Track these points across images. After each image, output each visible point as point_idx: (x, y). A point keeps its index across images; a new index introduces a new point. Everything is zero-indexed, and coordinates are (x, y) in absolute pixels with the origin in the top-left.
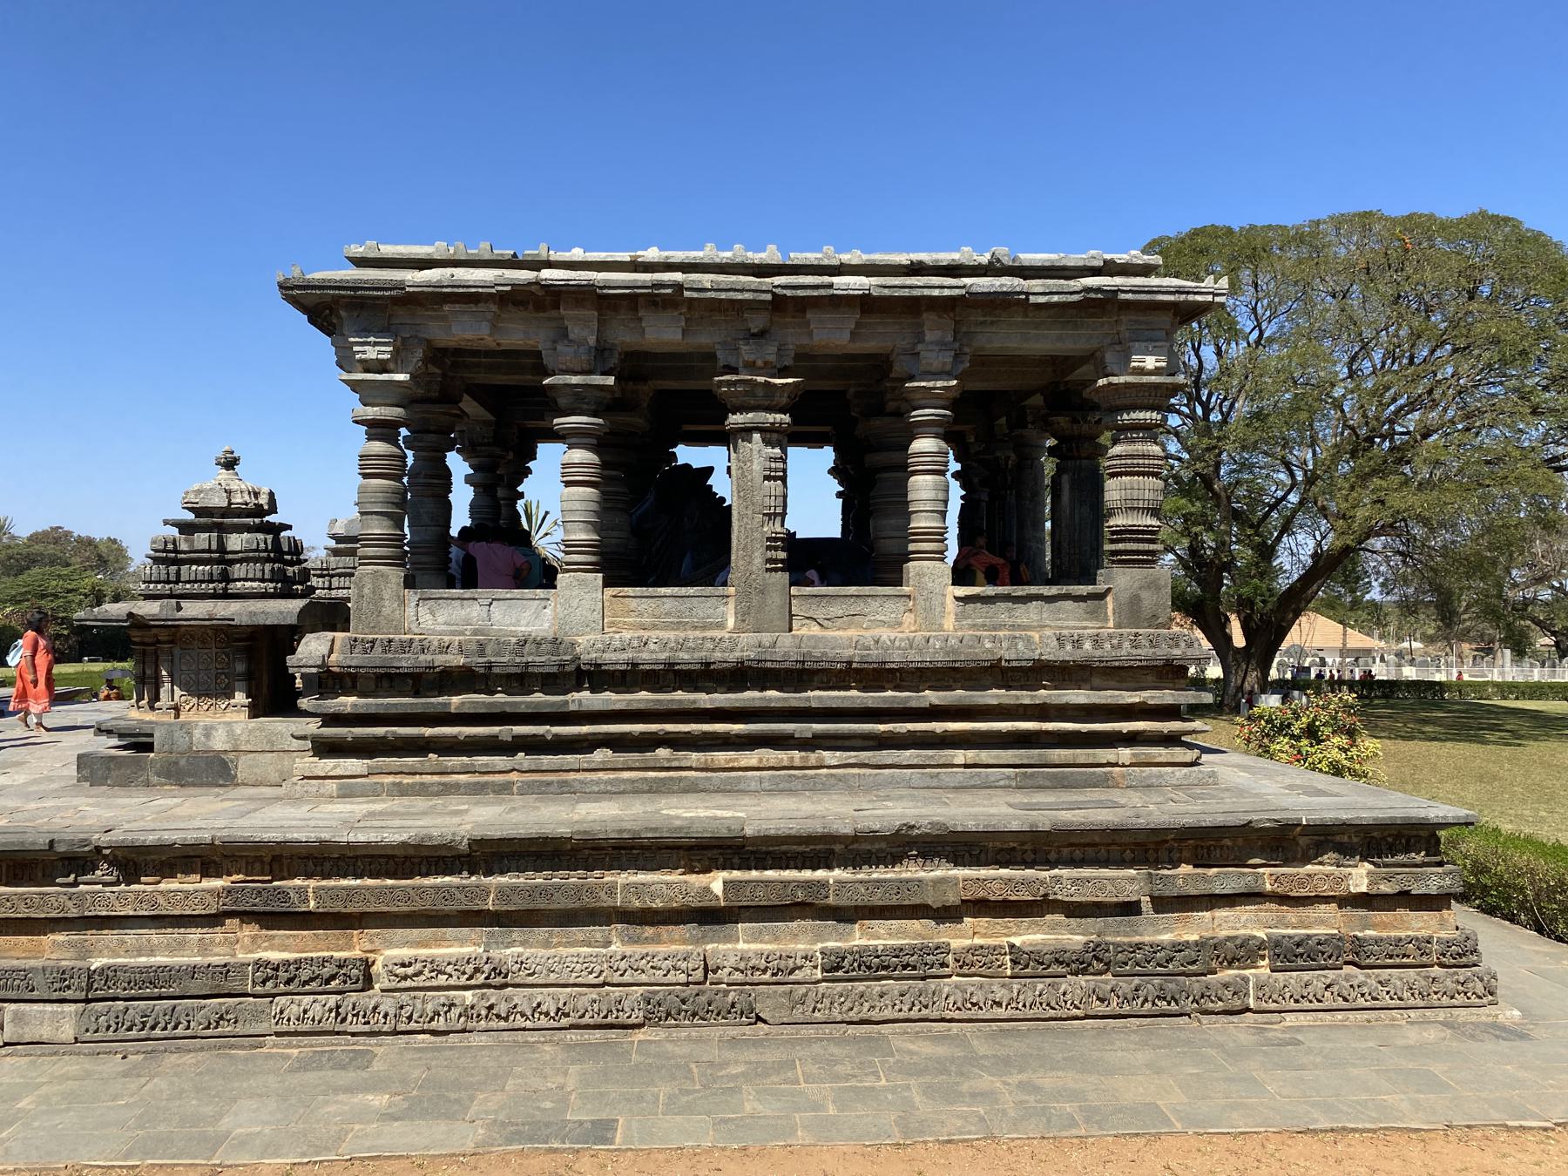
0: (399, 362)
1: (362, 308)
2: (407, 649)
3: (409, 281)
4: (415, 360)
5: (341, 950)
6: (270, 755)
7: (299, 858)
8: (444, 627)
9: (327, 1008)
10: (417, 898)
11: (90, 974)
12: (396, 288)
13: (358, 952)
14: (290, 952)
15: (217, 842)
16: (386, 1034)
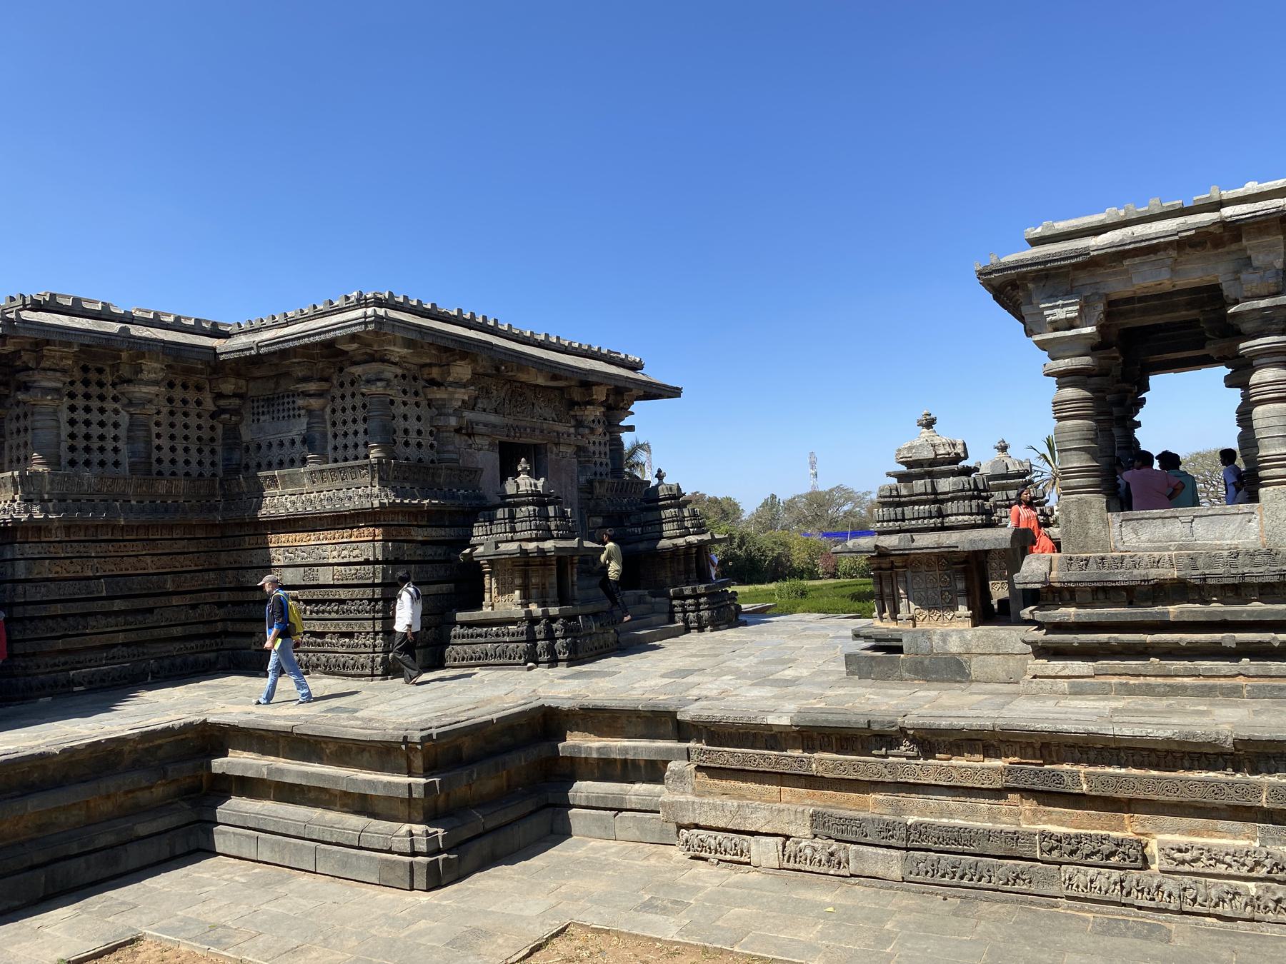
0: (1083, 318)
1: (1047, 278)
2: (1119, 565)
3: (1094, 246)
4: (1097, 314)
5: (1114, 830)
6: (997, 657)
7: (1065, 746)
8: (1149, 545)
9: (1112, 880)
10: (1186, 790)
11: (908, 828)
12: (1081, 255)
13: (1130, 834)
14: (1068, 827)
15: (997, 729)
16: (1172, 912)
